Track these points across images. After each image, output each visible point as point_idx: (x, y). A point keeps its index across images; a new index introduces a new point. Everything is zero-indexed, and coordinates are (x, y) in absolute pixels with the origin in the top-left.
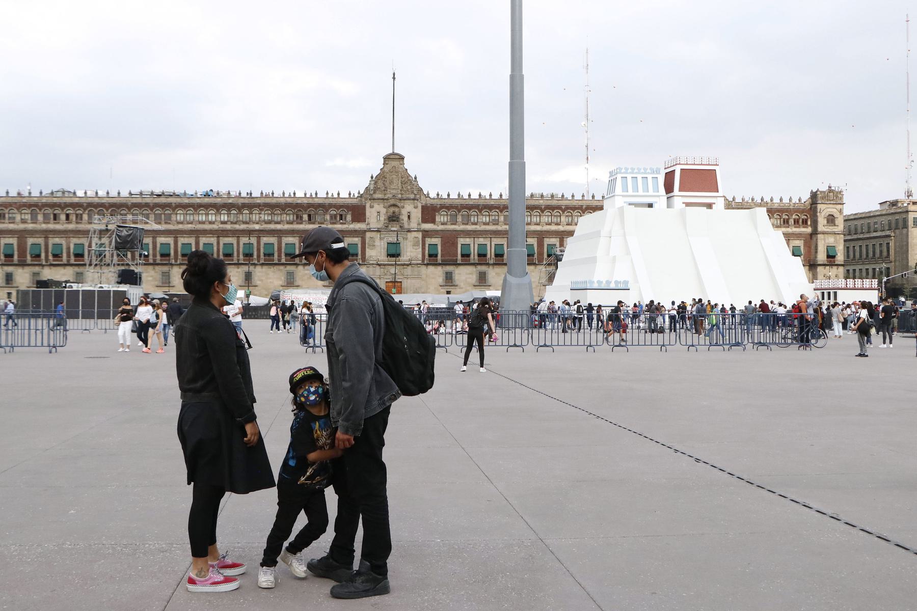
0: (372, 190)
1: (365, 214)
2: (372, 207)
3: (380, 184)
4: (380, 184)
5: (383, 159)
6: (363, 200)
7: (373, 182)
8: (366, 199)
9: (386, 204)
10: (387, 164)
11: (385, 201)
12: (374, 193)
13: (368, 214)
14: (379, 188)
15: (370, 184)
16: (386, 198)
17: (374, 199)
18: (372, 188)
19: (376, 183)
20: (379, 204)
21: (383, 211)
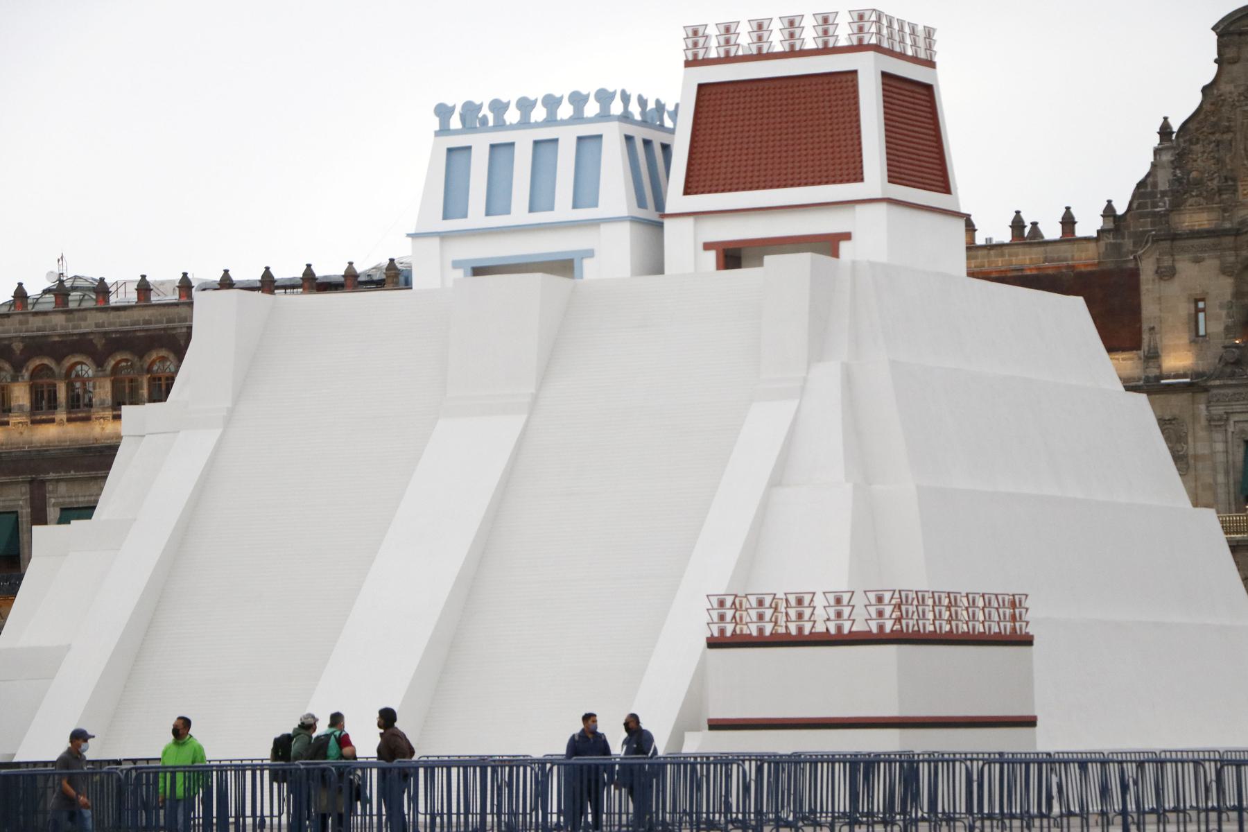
0: (1164, 194)
1: (1136, 311)
2: (1167, 274)
3: (1201, 162)
4: (1201, 162)
5: (1214, 37)
6: (1128, 243)
7: (1167, 157)
8: (1140, 240)
9: (1230, 258)
10: (1234, 61)
11: (1228, 241)
12: (1176, 206)
13: (1149, 309)
14: (1199, 183)
15: (1154, 165)
16: (1228, 225)
17: (1174, 237)
18: (1163, 186)
19: (1180, 159)
20: (1197, 261)
21: (1223, 288)
